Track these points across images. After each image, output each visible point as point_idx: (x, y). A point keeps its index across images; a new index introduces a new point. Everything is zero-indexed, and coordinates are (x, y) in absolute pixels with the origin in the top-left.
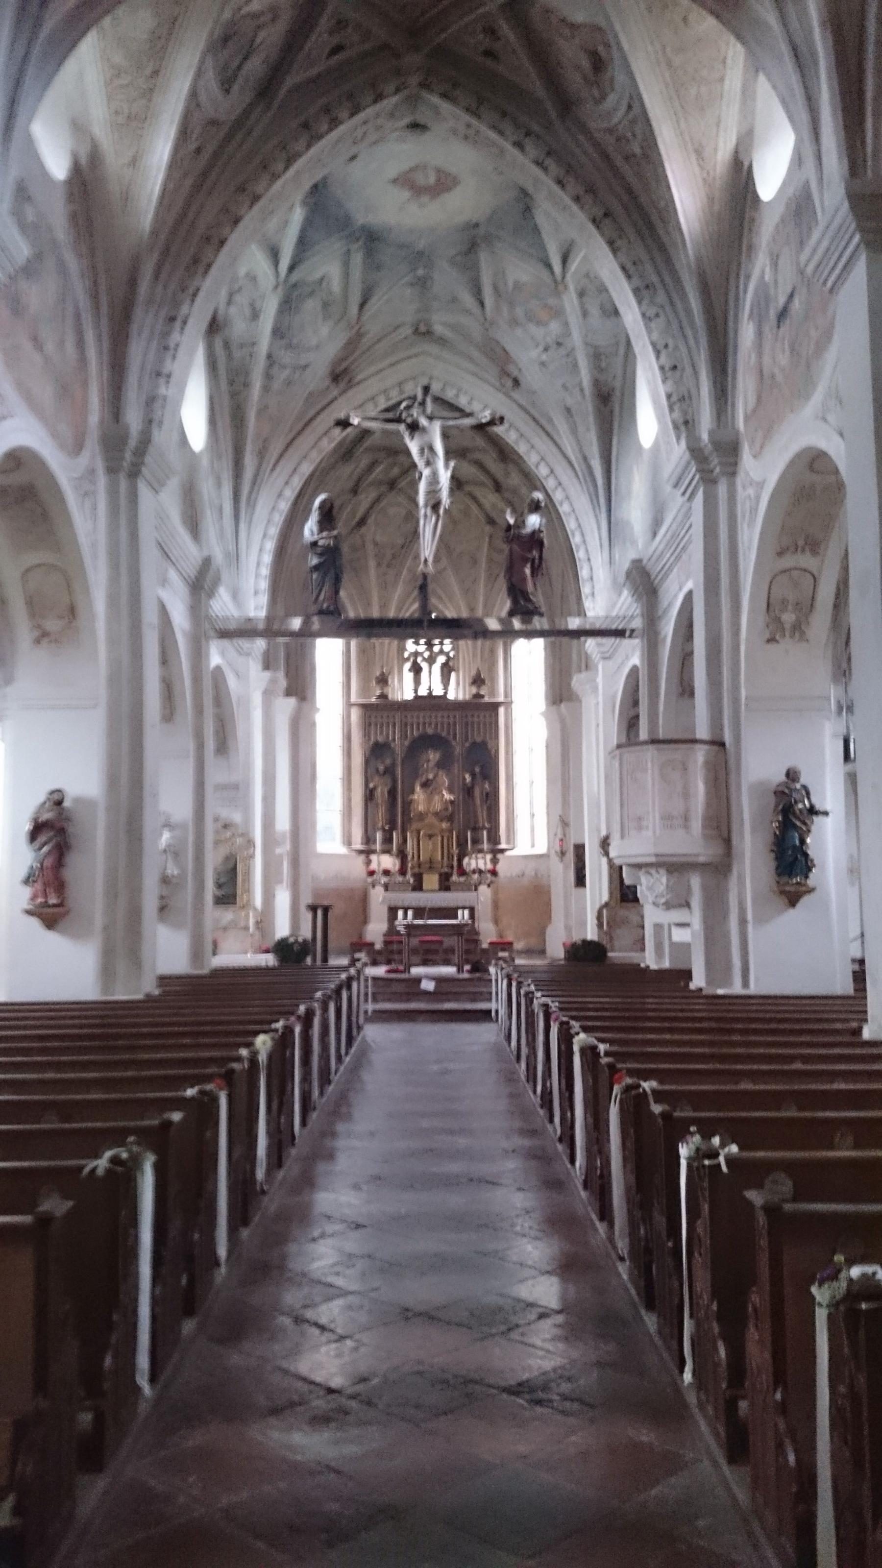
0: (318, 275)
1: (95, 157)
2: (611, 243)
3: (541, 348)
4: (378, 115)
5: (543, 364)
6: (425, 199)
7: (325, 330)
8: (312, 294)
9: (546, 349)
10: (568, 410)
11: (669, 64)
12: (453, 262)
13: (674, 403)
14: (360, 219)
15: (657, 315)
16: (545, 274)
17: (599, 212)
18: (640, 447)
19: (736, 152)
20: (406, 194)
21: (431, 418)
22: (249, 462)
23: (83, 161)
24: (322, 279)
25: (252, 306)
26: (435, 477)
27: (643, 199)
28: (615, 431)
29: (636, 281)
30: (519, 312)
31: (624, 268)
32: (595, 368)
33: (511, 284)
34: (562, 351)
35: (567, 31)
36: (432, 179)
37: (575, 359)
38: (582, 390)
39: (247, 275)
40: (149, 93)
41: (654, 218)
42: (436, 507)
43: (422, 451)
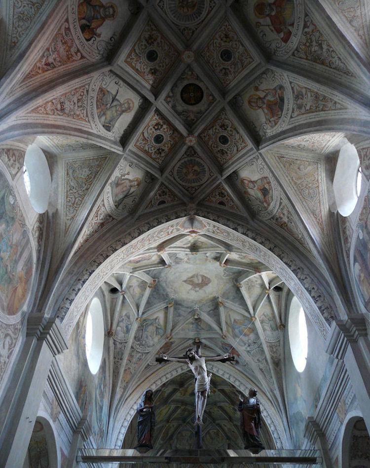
0: (155, 317)
1: (56, 214)
2: (279, 256)
3: (247, 345)
4: (178, 224)
5: (248, 352)
6: (197, 289)
7: (156, 339)
8: (152, 324)
9: (249, 346)
10: (261, 370)
11: (295, 183)
12: (209, 314)
13: (324, 310)
14: (172, 296)
15: (306, 278)
16: (246, 314)
17: (272, 246)
18: (298, 374)
19: (330, 210)
20: (190, 287)
21: (200, 357)
22: (119, 391)
23: (50, 214)
24: (156, 319)
25: (127, 327)
26: (203, 378)
27: (291, 239)
28: (283, 377)
29: (293, 267)
30: (237, 331)
31: (286, 264)
32: (271, 351)
33: (233, 320)
34: (256, 346)
35: (251, 185)
36: (200, 281)
37: (262, 348)
38: (266, 361)
39: (126, 315)
40: (83, 197)
41: (297, 244)
42: (203, 393)
43: (196, 369)
